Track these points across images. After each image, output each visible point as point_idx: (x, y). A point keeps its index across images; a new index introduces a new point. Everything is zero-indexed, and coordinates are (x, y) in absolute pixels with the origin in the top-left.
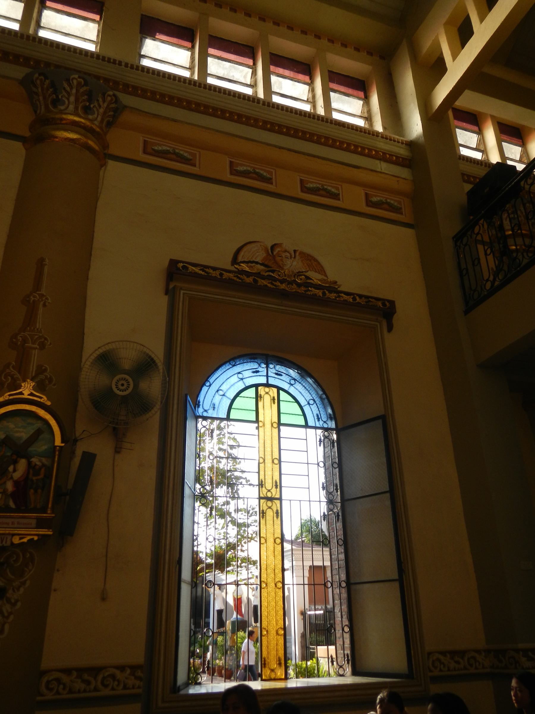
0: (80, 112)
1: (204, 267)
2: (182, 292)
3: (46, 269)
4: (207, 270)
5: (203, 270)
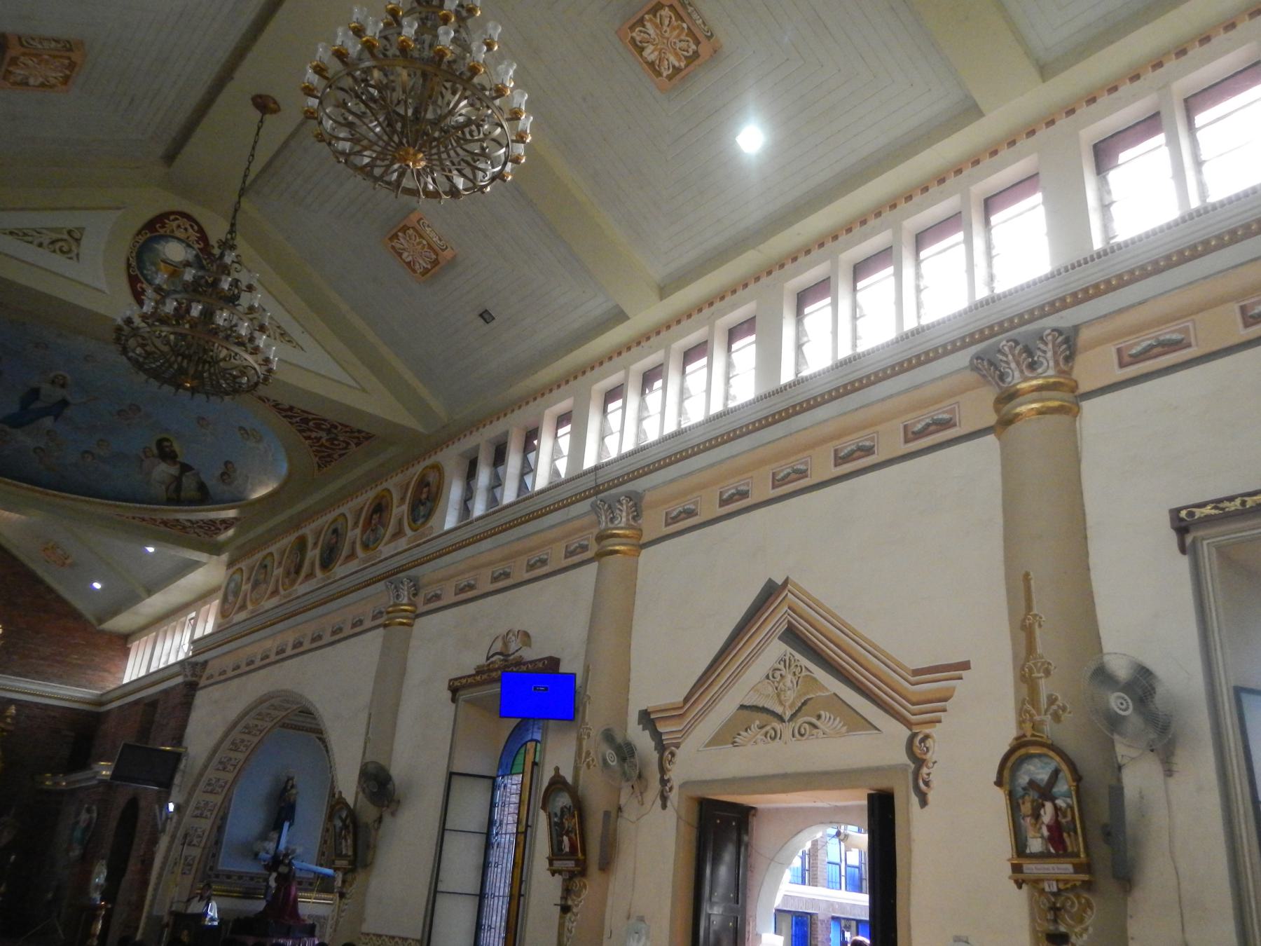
0: (1028, 374)
1: (1217, 502)
2: (1205, 542)
3: (1032, 582)
4: (1221, 505)
5: (1215, 508)
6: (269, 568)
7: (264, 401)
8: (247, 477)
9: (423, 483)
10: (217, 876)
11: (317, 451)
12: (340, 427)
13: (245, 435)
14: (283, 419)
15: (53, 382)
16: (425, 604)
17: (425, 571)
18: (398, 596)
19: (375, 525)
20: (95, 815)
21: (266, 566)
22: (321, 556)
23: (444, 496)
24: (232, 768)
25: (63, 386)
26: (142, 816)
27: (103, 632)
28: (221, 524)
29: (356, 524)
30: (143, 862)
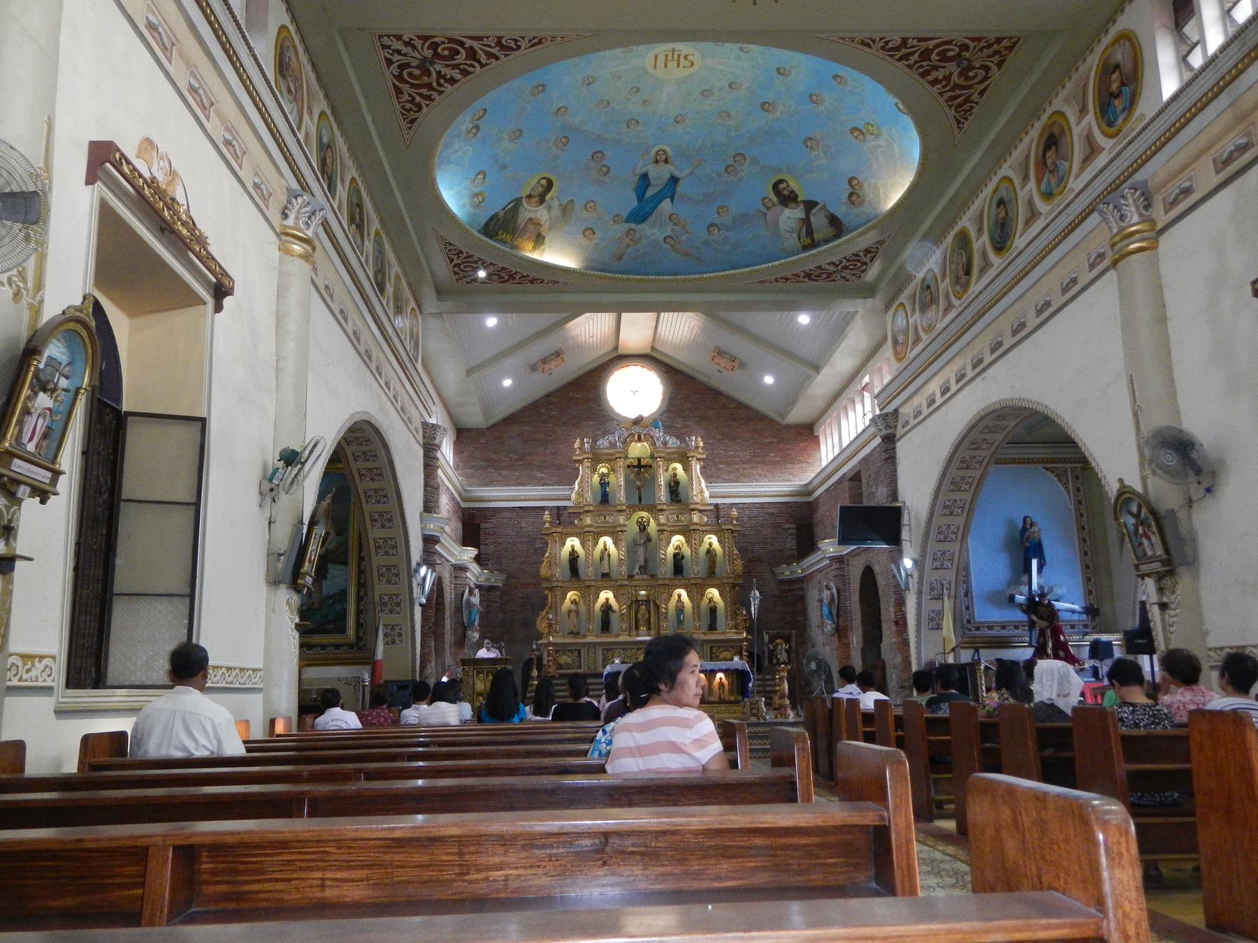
6: (933, 288)
7: (868, 45)
8: (875, 184)
9: (1109, 69)
10: (977, 629)
11: (952, 99)
12: (972, 45)
13: (861, 136)
14: (897, 63)
15: (657, 161)
16: (1166, 212)
17: (1152, 171)
18: (1122, 218)
19: (1054, 163)
20: (835, 591)
21: (928, 287)
22: (992, 239)
23: (1147, 71)
24: (959, 511)
25: (666, 161)
26: (881, 581)
27: (789, 427)
28: (865, 256)
29: (1026, 178)
30: (896, 623)
